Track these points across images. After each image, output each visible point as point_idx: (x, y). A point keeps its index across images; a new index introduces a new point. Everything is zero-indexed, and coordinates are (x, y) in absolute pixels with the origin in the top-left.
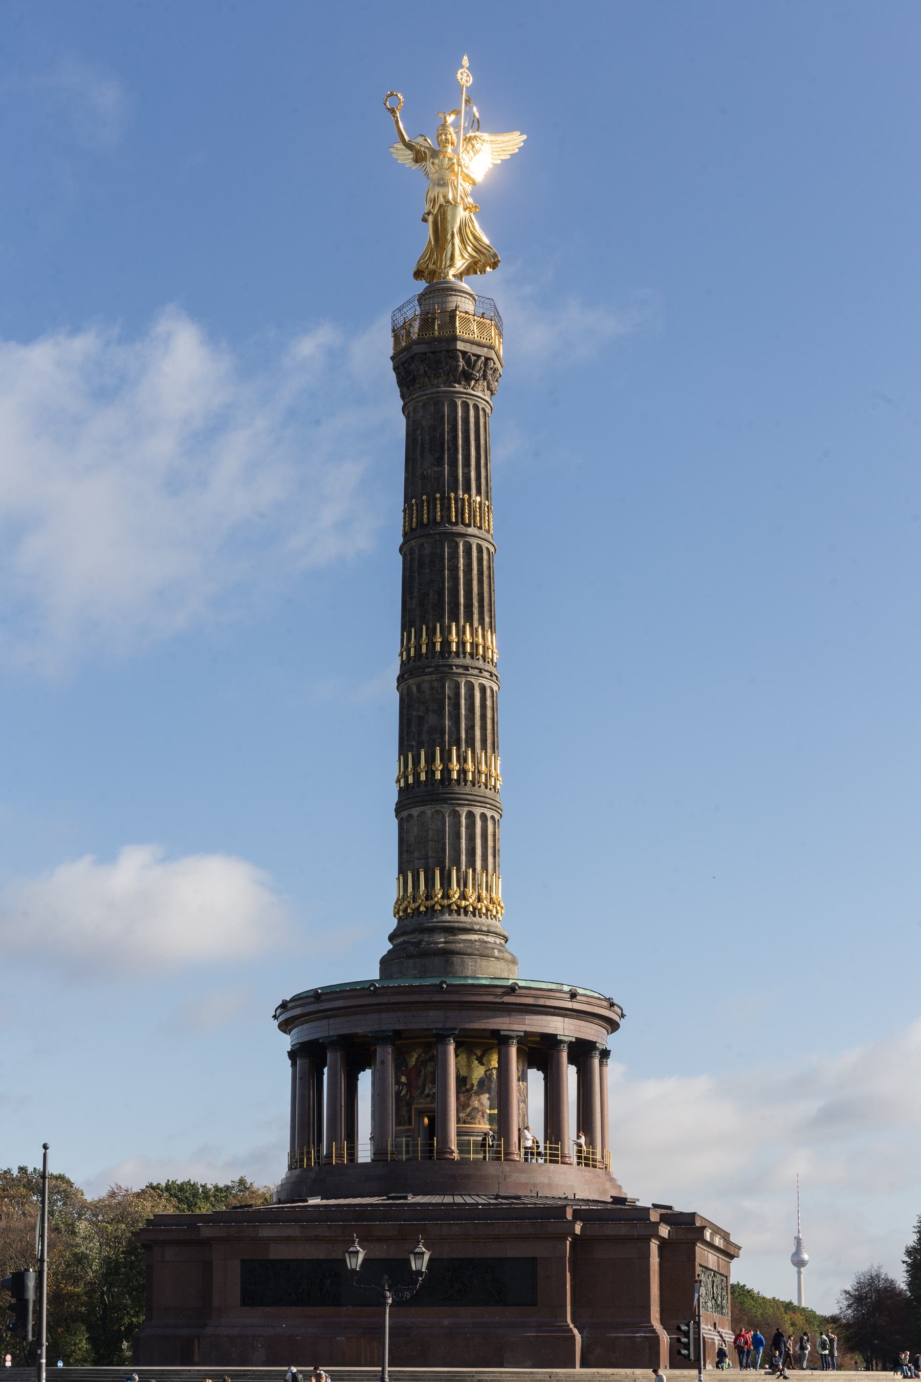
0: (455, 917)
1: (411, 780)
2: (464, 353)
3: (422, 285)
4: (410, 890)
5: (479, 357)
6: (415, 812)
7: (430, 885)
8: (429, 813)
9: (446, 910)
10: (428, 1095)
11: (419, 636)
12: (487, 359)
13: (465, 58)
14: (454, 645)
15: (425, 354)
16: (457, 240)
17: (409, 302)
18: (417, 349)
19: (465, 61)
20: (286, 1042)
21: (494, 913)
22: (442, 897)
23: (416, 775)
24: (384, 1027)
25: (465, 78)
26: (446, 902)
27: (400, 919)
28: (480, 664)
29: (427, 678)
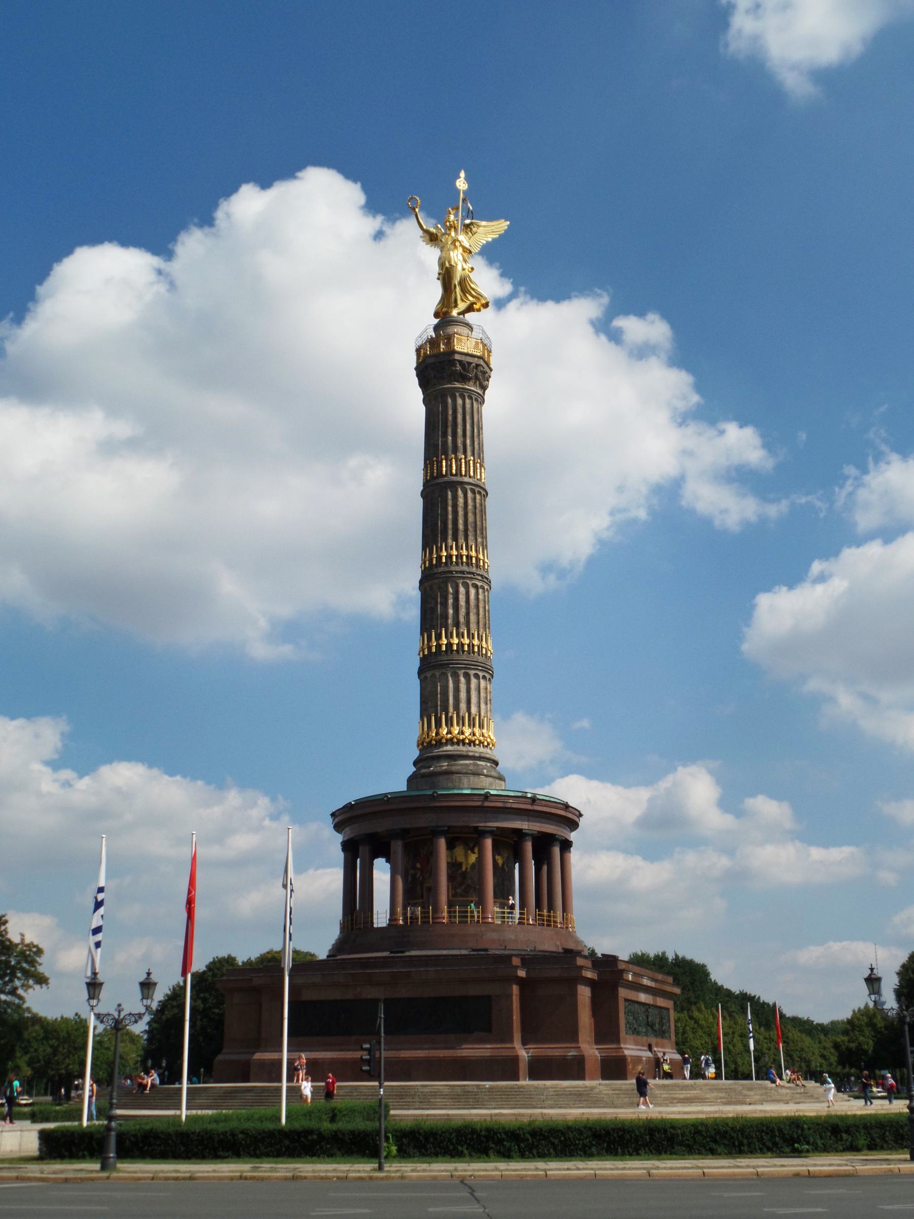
0: (456, 747)
2: (460, 362)
3: (436, 321)
4: (426, 729)
5: (471, 363)
6: (429, 675)
8: (437, 674)
11: (431, 553)
12: (478, 365)
16: (458, 289)
18: (429, 361)
19: (462, 174)
20: (339, 838)
23: (430, 648)
25: (461, 184)
27: (420, 750)
28: (474, 570)
29: (436, 581)
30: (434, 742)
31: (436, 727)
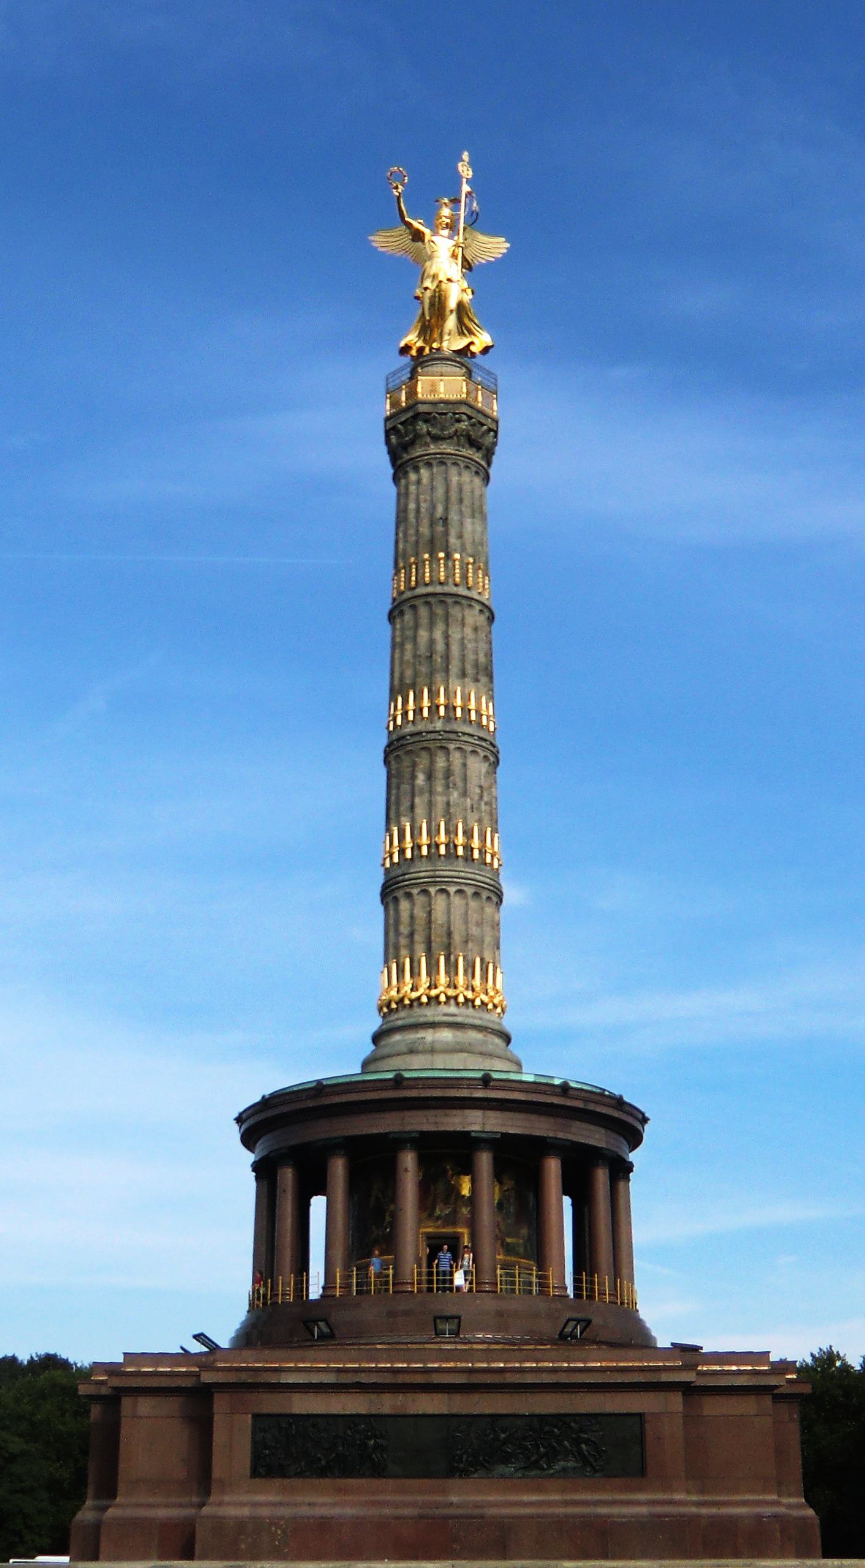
1: (409, 855)
2: (470, 418)
5: (483, 425)
7: (433, 973)
9: (452, 1001)
10: (438, 1218)
11: (418, 698)
12: (490, 430)
13: (466, 153)
14: (459, 713)
15: (430, 414)
17: (402, 369)
18: (422, 408)
19: (466, 156)
21: (499, 1010)
22: (449, 986)
24: (408, 1128)
25: (465, 171)
26: (451, 992)
30: (424, 999)
31: (429, 974)
